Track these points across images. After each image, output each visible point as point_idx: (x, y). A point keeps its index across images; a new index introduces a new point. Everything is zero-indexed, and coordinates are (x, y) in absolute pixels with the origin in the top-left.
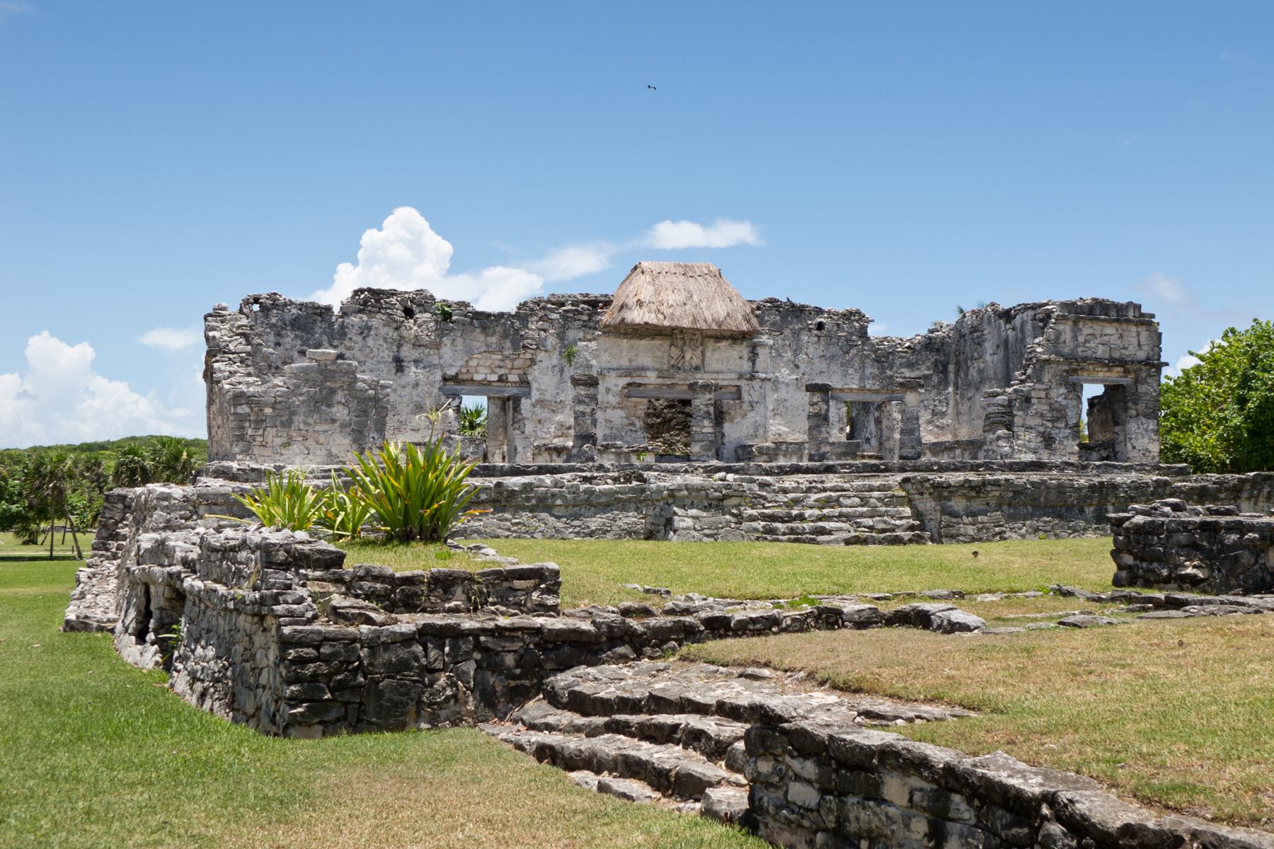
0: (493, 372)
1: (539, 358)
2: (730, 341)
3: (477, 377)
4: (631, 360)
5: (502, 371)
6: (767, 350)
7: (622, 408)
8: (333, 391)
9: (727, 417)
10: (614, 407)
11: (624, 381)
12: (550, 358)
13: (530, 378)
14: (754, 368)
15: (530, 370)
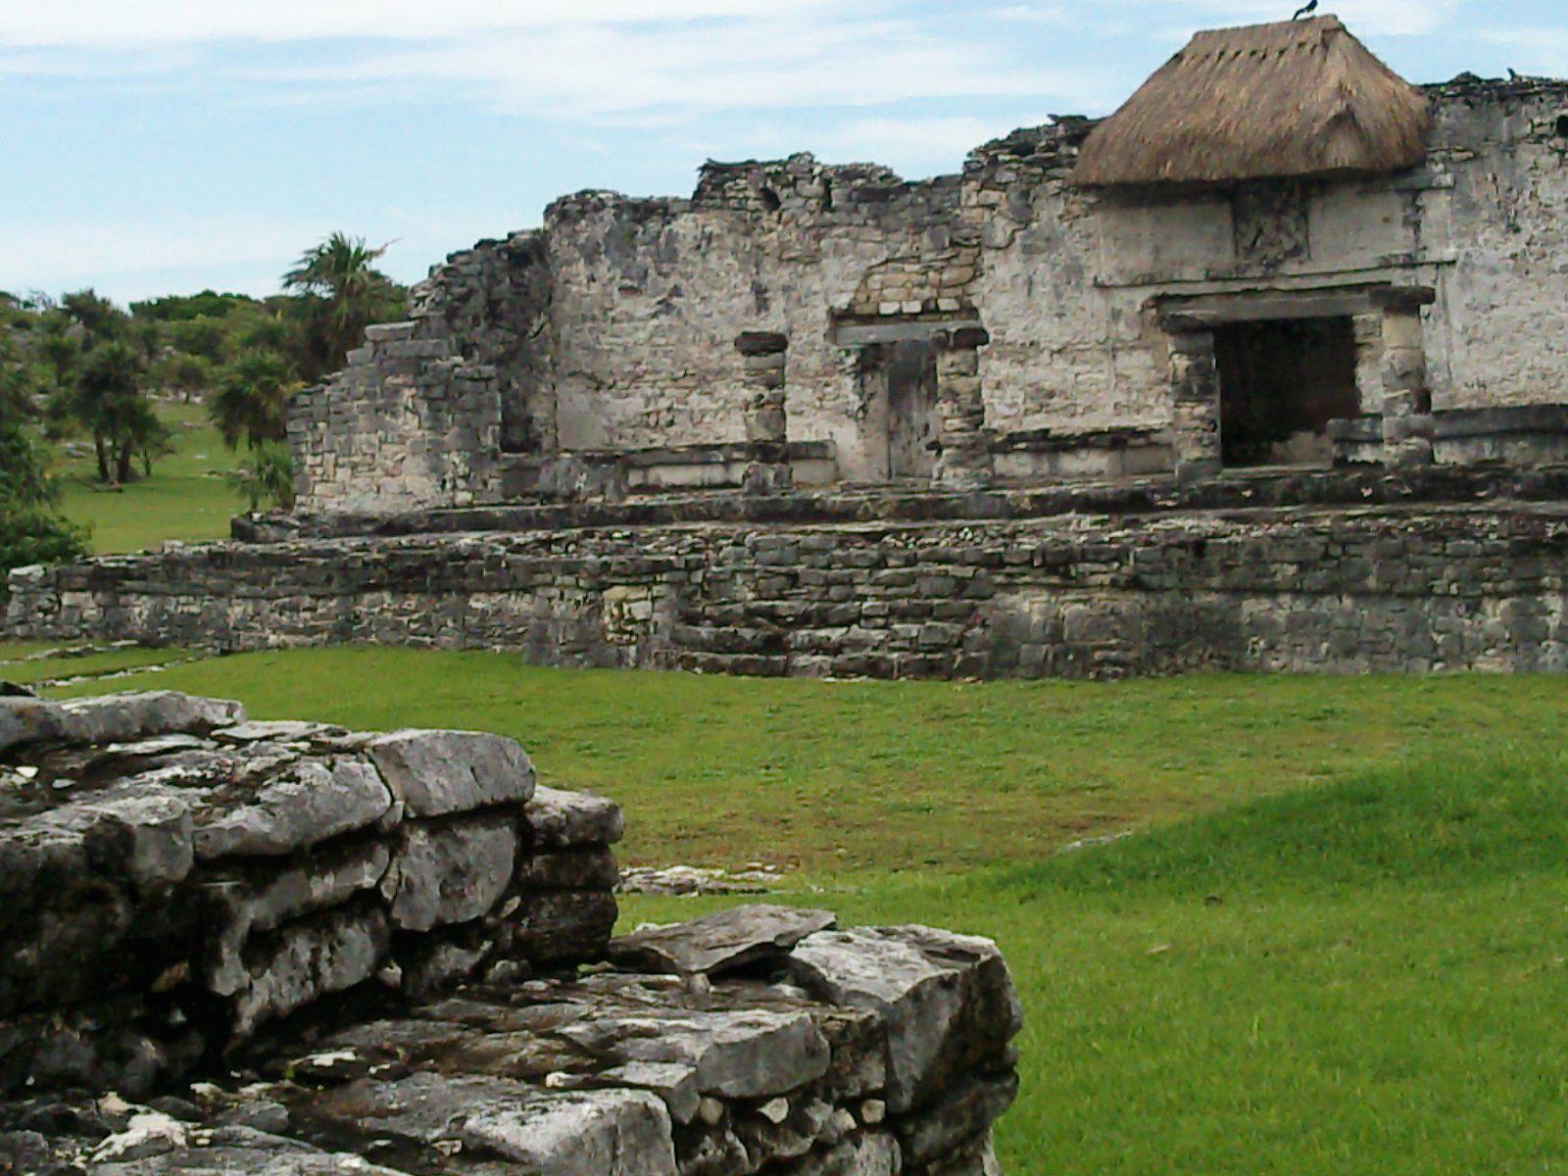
0: (910, 297)
1: (986, 264)
2: (1359, 187)
3: (888, 308)
4: (1157, 251)
5: (927, 293)
6: (1443, 199)
7: (1147, 348)
8: (396, 391)
9: (1365, 353)
10: (1133, 348)
11: (1142, 296)
12: (1006, 261)
13: (975, 302)
14: (1417, 240)
15: (974, 287)
